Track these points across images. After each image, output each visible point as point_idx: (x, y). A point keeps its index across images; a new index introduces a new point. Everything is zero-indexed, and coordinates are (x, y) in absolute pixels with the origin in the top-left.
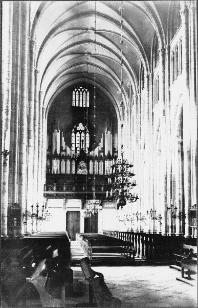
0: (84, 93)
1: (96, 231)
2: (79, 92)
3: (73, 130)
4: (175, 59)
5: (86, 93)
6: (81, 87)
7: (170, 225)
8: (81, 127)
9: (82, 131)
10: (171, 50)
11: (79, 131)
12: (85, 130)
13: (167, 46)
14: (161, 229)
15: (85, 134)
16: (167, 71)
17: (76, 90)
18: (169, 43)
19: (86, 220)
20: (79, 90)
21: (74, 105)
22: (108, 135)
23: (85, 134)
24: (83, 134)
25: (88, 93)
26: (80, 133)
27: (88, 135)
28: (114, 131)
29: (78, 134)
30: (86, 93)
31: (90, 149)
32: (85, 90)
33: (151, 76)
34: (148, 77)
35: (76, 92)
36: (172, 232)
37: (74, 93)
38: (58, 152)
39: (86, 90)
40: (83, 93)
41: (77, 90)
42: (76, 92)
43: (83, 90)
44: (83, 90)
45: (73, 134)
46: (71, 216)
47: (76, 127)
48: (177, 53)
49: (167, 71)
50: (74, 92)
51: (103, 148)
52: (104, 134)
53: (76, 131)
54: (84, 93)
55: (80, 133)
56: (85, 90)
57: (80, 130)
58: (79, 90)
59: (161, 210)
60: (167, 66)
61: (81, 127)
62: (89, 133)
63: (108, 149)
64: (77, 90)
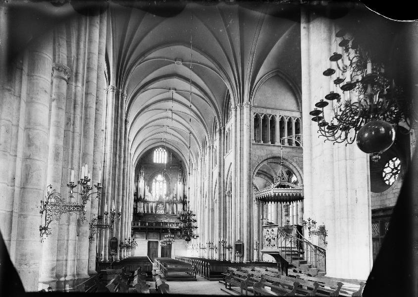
6: (161, 148)
7: (222, 253)
8: (160, 177)
12: (164, 180)
14: (216, 257)
15: (163, 183)
19: (163, 248)
21: (154, 162)
22: (179, 186)
23: (163, 183)
24: (161, 183)
31: (167, 195)
33: (211, 147)
34: (210, 147)
36: (224, 258)
38: (143, 197)
40: (162, 152)
45: (154, 183)
46: (151, 244)
51: (176, 195)
52: (177, 184)
53: (156, 181)
58: (159, 150)
59: (216, 243)
64: (158, 150)
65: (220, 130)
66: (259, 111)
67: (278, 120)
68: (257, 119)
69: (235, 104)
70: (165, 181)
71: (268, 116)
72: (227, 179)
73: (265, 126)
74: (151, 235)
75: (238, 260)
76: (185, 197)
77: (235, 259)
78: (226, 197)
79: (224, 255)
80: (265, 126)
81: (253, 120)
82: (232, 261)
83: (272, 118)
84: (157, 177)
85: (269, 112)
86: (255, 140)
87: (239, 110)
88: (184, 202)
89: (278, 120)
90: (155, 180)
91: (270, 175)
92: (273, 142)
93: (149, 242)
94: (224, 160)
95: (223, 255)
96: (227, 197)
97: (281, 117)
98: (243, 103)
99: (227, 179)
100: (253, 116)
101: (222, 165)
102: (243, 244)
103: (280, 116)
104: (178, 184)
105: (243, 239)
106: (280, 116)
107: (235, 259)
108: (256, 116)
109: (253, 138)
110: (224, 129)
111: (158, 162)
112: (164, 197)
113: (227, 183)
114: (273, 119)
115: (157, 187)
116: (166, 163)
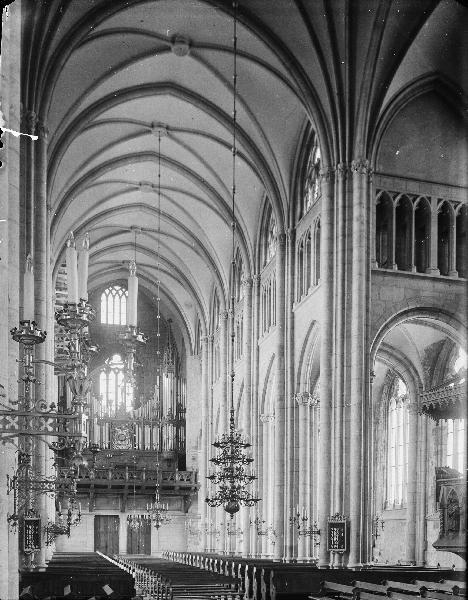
1: (148, 550)
2: (114, 296)
4: (305, 255)
6: (117, 288)
7: (288, 544)
8: (117, 358)
9: (119, 370)
10: (298, 238)
13: (289, 231)
16: (288, 277)
17: (107, 291)
18: (294, 225)
19: (130, 531)
21: (103, 321)
24: (121, 376)
26: (117, 374)
28: (179, 376)
31: (137, 405)
33: (255, 281)
34: (251, 282)
35: (107, 296)
36: (292, 556)
37: (103, 296)
41: (111, 291)
42: (107, 296)
44: (121, 292)
45: (103, 376)
48: (309, 245)
49: (288, 277)
50: (104, 295)
52: (161, 378)
53: (108, 371)
55: (117, 374)
58: (114, 292)
60: (288, 269)
61: (117, 358)
63: (168, 404)
64: (111, 291)
65: (283, 236)
66: (388, 185)
67: (435, 209)
68: (382, 209)
69: (330, 166)
71: (411, 199)
72: (301, 362)
73: (402, 228)
74: (101, 501)
75: (334, 563)
76: (180, 409)
77: (328, 559)
78: (297, 407)
79: (293, 549)
80: (402, 228)
81: (373, 209)
82: (320, 564)
83: (419, 204)
85: (413, 188)
86: (378, 260)
87: (340, 180)
88: (179, 423)
89: (435, 209)
91: (402, 354)
92: (422, 266)
93: (97, 518)
94: (293, 313)
95: (291, 548)
96: (301, 408)
97: (441, 204)
98: (350, 161)
99: (301, 362)
100: (374, 200)
101: (287, 327)
102: (349, 523)
103: (440, 200)
104: (164, 378)
105: (348, 511)
106: (440, 200)
107: (328, 559)
108: (381, 199)
109: (373, 255)
110: (294, 233)
111: (110, 322)
112: (129, 409)
113: (299, 373)
114: (423, 205)
115: (112, 383)
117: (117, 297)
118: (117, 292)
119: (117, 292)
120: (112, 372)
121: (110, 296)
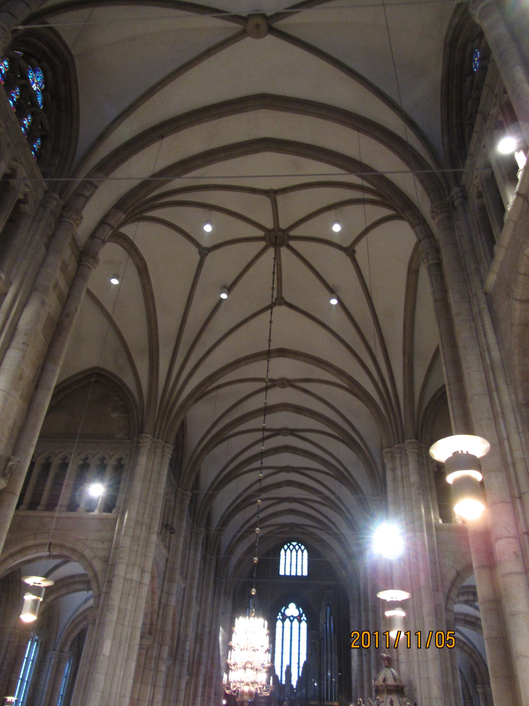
0: (300, 552)
2: (291, 551)
3: (280, 616)
5: (302, 551)
6: (294, 543)
8: (292, 610)
9: (294, 618)
11: (289, 617)
12: (300, 615)
15: (300, 621)
17: (286, 547)
20: (291, 547)
21: (282, 573)
23: (300, 621)
24: (296, 622)
25: (305, 552)
26: (292, 621)
27: (304, 625)
29: (287, 621)
30: (302, 551)
32: (300, 547)
35: (286, 551)
37: (282, 552)
39: (303, 547)
41: (289, 547)
42: (286, 551)
43: (297, 547)
44: (297, 547)
47: (284, 610)
54: (300, 552)
55: (292, 621)
56: (300, 547)
57: (292, 616)
58: (291, 547)
61: (292, 610)
62: (306, 622)
64: (289, 547)
70: (304, 617)
84: (287, 607)
90: (283, 615)
116: (305, 573)
117: (294, 551)
118: (294, 547)
119: (294, 547)
120: (287, 620)
121: (288, 551)
